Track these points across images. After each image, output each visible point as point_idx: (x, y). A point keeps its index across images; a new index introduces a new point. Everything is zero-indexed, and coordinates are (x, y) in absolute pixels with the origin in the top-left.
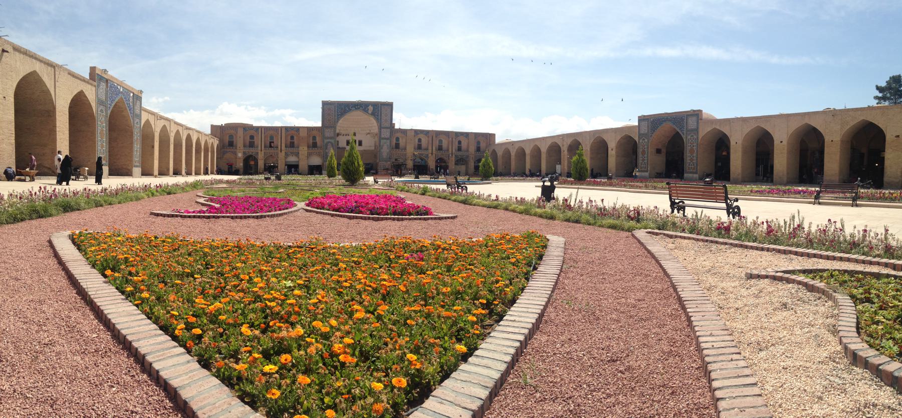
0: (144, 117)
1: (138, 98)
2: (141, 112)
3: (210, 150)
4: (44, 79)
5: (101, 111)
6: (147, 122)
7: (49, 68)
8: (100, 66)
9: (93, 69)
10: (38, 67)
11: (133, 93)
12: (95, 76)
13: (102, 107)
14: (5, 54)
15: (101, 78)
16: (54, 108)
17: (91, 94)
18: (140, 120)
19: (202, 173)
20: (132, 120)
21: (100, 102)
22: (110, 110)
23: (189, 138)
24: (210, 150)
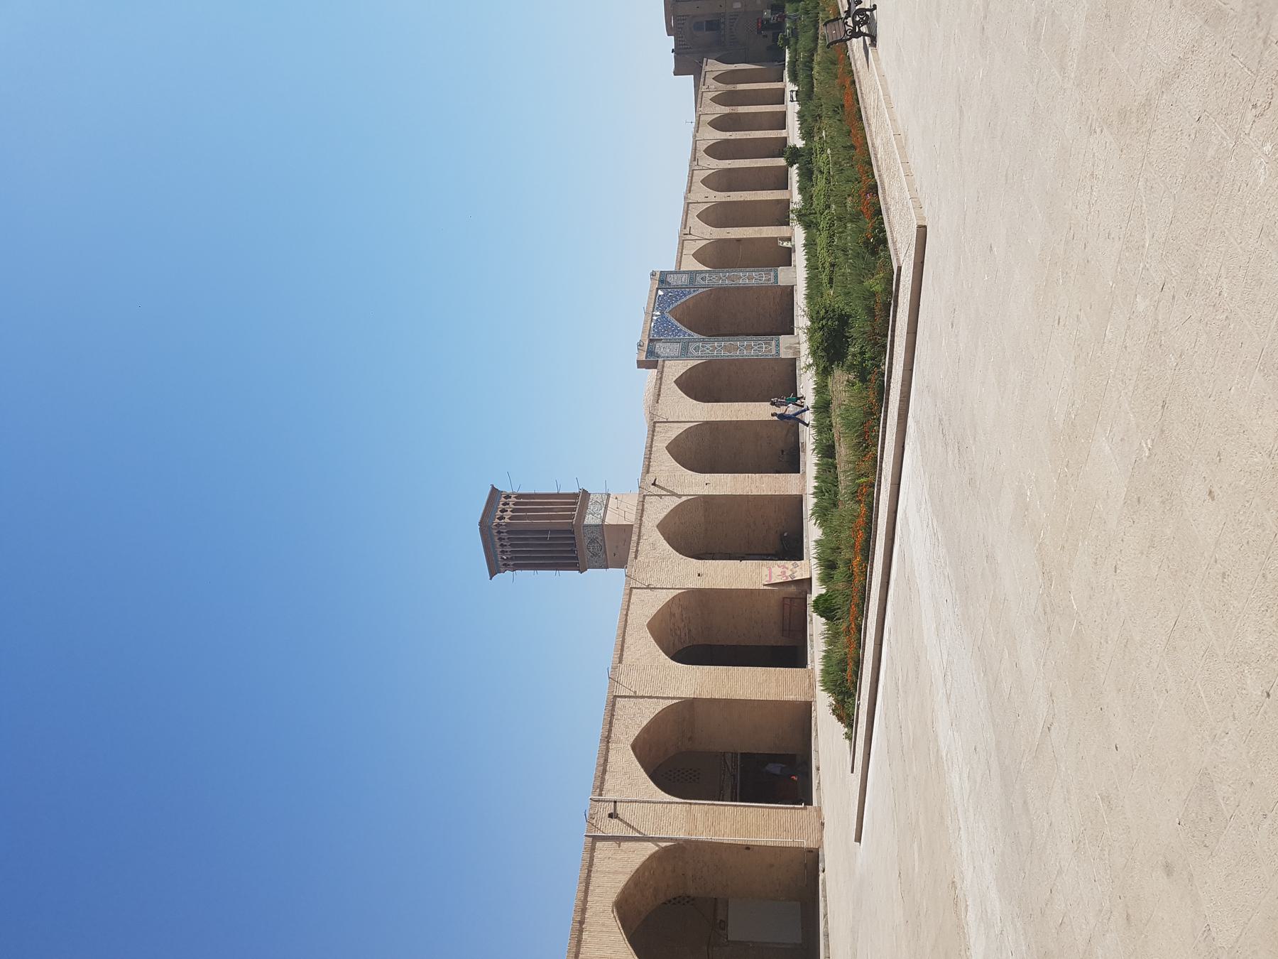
0: (692, 264)
1: (663, 279)
2: (684, 272)
3: (730, 87)
4: (674, 437)
5: (697, 349)
6: (698, 256)
7: (657, 429)
8: (634, 355)
9: (641, 364)
10: (661, 444)
11: (658, 289)
12: (650, 361)
13: (691, 349)
14: (657, 483)
15: (651, 352)
16: (707, 422)
17: (677, 368)
18: (697, 272)
19: (777, 108)
20: (701, 290)
21: (684, 354)
22: (692, 333)
23: (716, 151)
24: (730, 87)
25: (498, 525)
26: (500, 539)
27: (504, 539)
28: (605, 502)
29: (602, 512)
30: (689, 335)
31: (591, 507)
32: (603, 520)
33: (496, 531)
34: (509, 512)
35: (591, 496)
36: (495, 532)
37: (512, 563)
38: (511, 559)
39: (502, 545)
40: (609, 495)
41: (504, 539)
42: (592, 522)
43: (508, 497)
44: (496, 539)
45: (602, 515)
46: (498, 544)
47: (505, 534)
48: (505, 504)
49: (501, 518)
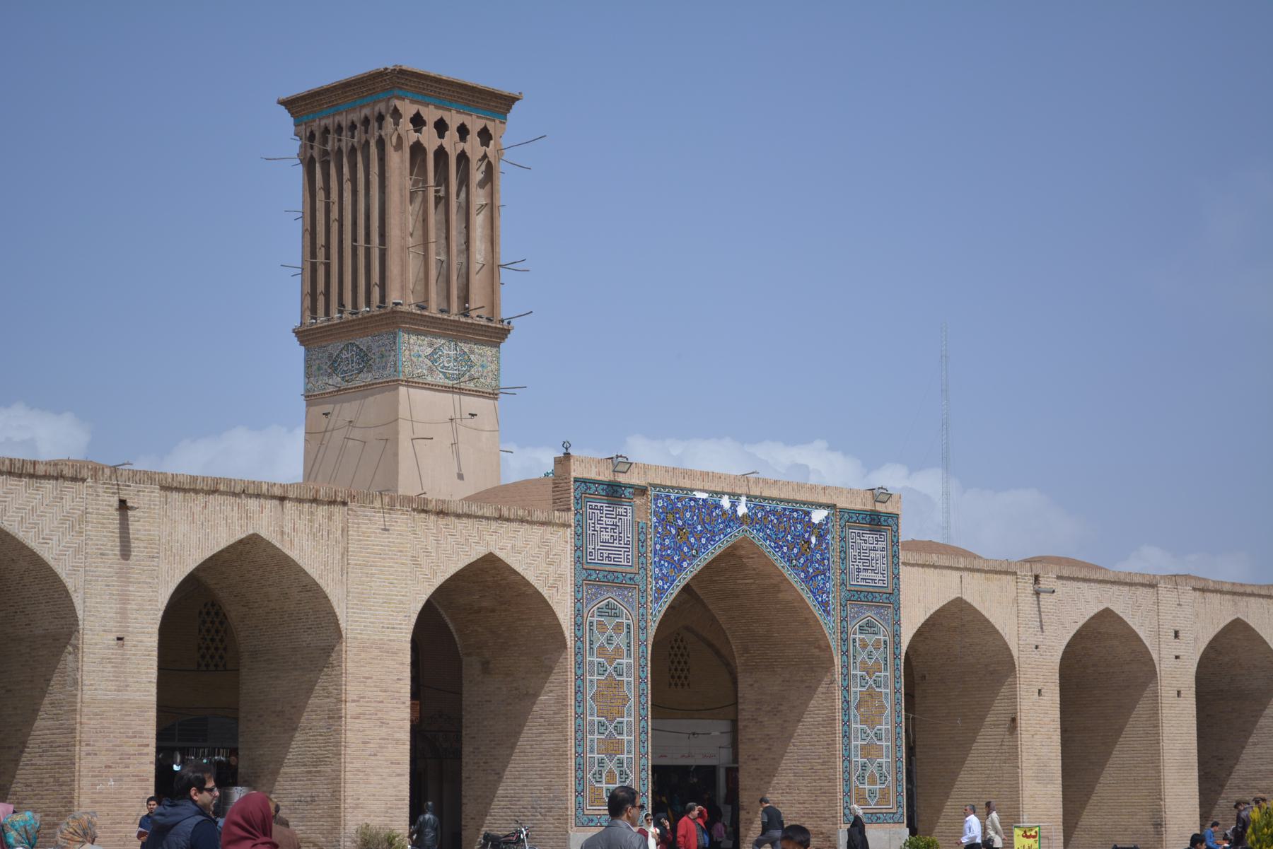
25: (396, 114)
26: (366, 121)
27: (366, 132)
28: (471, 385)
29: (439, 379)
30: (660, 592)
31: (448, 350)
32: (409, 383)
33: (383, 111)
34: (438, 142)
35: (489, 351)
36: (381, 107)
37: (316, 155)
38: (326, 153)
39: (353, 127)
40: (493, 396)
41: (366, 132)
42: (404, 356)
43: (485, 136)
44: (366, 111)
45: (429, 379)
46: (357, 116)
47: (377, 134)
48: (463, 131)
49: (418, 121)
